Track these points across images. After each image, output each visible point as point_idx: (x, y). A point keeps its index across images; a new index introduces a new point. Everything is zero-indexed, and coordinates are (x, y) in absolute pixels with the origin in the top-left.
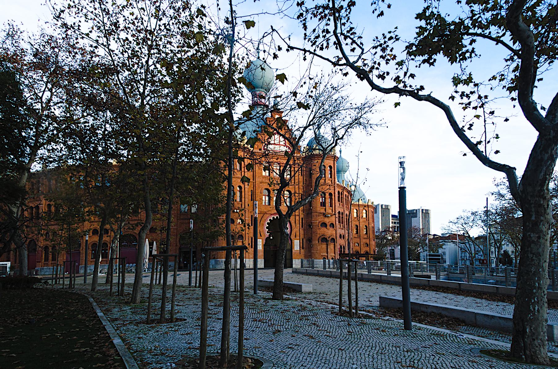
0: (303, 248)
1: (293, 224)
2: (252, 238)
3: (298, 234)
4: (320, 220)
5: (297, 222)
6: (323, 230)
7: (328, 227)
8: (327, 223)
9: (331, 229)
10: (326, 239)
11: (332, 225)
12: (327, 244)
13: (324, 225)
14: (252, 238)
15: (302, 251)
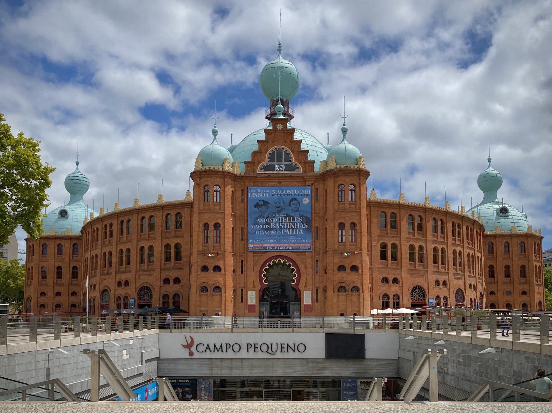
0: (317, 301)
1: (302, 269)
2: (242, 290)
3: (309, 282)
4: (336, 261)
5: (309, 267)
6: (342, 275)
7: (348, 270)
8: (346, 266)
9: (353, 273)
10: (344, 287)
11: (354, 268)
12: (347, 295)
13: (342, 268)
14: (242, 290)
15: (316, 304)
